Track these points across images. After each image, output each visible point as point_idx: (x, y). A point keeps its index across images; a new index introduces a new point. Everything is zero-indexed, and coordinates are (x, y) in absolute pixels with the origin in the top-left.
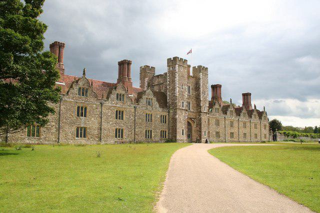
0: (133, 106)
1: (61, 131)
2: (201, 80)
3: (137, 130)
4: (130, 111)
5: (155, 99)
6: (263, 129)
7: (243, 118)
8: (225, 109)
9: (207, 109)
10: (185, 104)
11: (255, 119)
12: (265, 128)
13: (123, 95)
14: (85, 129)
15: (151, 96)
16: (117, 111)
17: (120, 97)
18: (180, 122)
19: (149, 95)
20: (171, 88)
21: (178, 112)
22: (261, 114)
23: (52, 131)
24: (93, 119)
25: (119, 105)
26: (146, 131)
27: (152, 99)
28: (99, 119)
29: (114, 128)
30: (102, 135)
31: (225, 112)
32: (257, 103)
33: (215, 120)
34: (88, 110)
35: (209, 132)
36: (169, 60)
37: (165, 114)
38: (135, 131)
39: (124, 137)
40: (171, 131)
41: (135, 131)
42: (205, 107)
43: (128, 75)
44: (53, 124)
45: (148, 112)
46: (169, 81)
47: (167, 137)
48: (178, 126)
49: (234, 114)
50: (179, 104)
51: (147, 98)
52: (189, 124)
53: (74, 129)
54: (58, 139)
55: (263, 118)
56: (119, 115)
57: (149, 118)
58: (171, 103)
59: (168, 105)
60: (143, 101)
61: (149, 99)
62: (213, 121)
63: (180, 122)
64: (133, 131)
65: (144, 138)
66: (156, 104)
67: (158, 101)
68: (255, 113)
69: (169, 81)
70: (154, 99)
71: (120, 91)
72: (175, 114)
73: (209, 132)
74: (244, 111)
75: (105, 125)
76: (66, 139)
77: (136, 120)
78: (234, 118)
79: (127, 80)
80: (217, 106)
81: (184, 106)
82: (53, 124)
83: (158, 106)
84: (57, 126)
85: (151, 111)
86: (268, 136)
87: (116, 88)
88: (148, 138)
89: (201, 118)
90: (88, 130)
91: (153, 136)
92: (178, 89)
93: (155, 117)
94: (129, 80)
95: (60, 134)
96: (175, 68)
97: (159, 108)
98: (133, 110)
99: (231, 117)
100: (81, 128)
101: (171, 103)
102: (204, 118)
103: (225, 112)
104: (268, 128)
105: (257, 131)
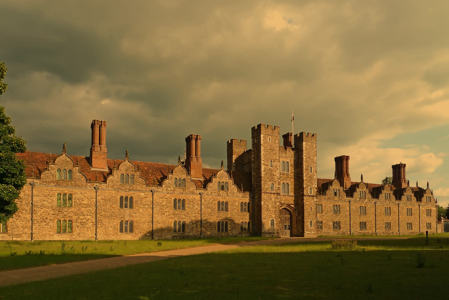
0: (198, 191)
1: (99, 226)
2: (304, 152)
4: (194, 199)
11: (408, 202)
17: (181, 184)
19: (221, 177)
22: (419, 193)
25: (178, 190)
34: (134, 200)
42: (310, 188)
44: (89, 217)
53: (117, 222)
55: (424, 199)
66: (233, 188)
67: (237, 183)
68: (408, 193)
82: (89, 217)
84: (94, 221)
86: (434, 224)
87: (172, 172)
88: (222, 230)
89: (303, 204)
98: (198, 197)
101: (255, 186)
102: (309, 203)
105: (411, 219)
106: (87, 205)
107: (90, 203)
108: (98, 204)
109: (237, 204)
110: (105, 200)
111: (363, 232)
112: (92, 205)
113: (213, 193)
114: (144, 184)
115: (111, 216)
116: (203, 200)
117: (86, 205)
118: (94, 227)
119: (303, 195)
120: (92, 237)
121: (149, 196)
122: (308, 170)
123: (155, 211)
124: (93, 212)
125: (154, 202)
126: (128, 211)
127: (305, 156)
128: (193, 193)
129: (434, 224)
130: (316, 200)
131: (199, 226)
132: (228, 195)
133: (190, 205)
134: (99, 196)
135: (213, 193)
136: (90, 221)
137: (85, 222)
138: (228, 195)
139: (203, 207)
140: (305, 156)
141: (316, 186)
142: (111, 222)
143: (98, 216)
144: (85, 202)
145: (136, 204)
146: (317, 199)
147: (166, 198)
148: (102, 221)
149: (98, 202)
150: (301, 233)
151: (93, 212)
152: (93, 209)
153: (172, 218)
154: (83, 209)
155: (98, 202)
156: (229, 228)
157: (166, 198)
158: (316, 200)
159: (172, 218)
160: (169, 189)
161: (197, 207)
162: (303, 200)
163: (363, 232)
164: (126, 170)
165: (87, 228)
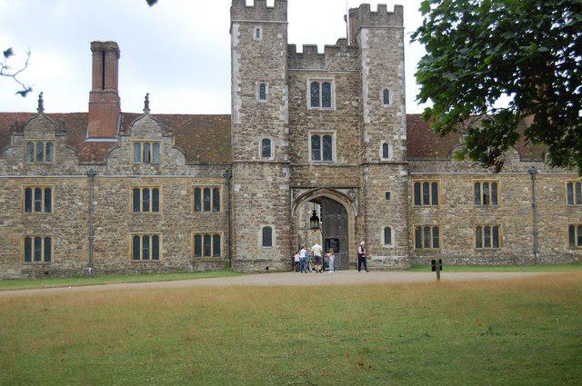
0: (84, 170)
5: (171, 142)
13: (49, 145)
16: (28, 191)
26: (136, 239)
27: (156, 144)
29: (20, 238)
37: (211, 183)
45: (141, 184)
51: (137, 144)
57: (145, 200)
61: (147, 144)
64: (85, 241)
65: (128, 258)
77: (97, 209)
83: (181, 161)
85: (151, 180)
91: (162, 251)
93: (171, 196)
97: (187, 167)
113: (123, 172)
128: (70, 172)
131: (85, 247)
132: (159, 173)
135: (123, 172)
141: (404, 137)
147: (7, 189)
153: (20, 231)
156: (165, 251)
157: (7, 189)
159: (20, 231)
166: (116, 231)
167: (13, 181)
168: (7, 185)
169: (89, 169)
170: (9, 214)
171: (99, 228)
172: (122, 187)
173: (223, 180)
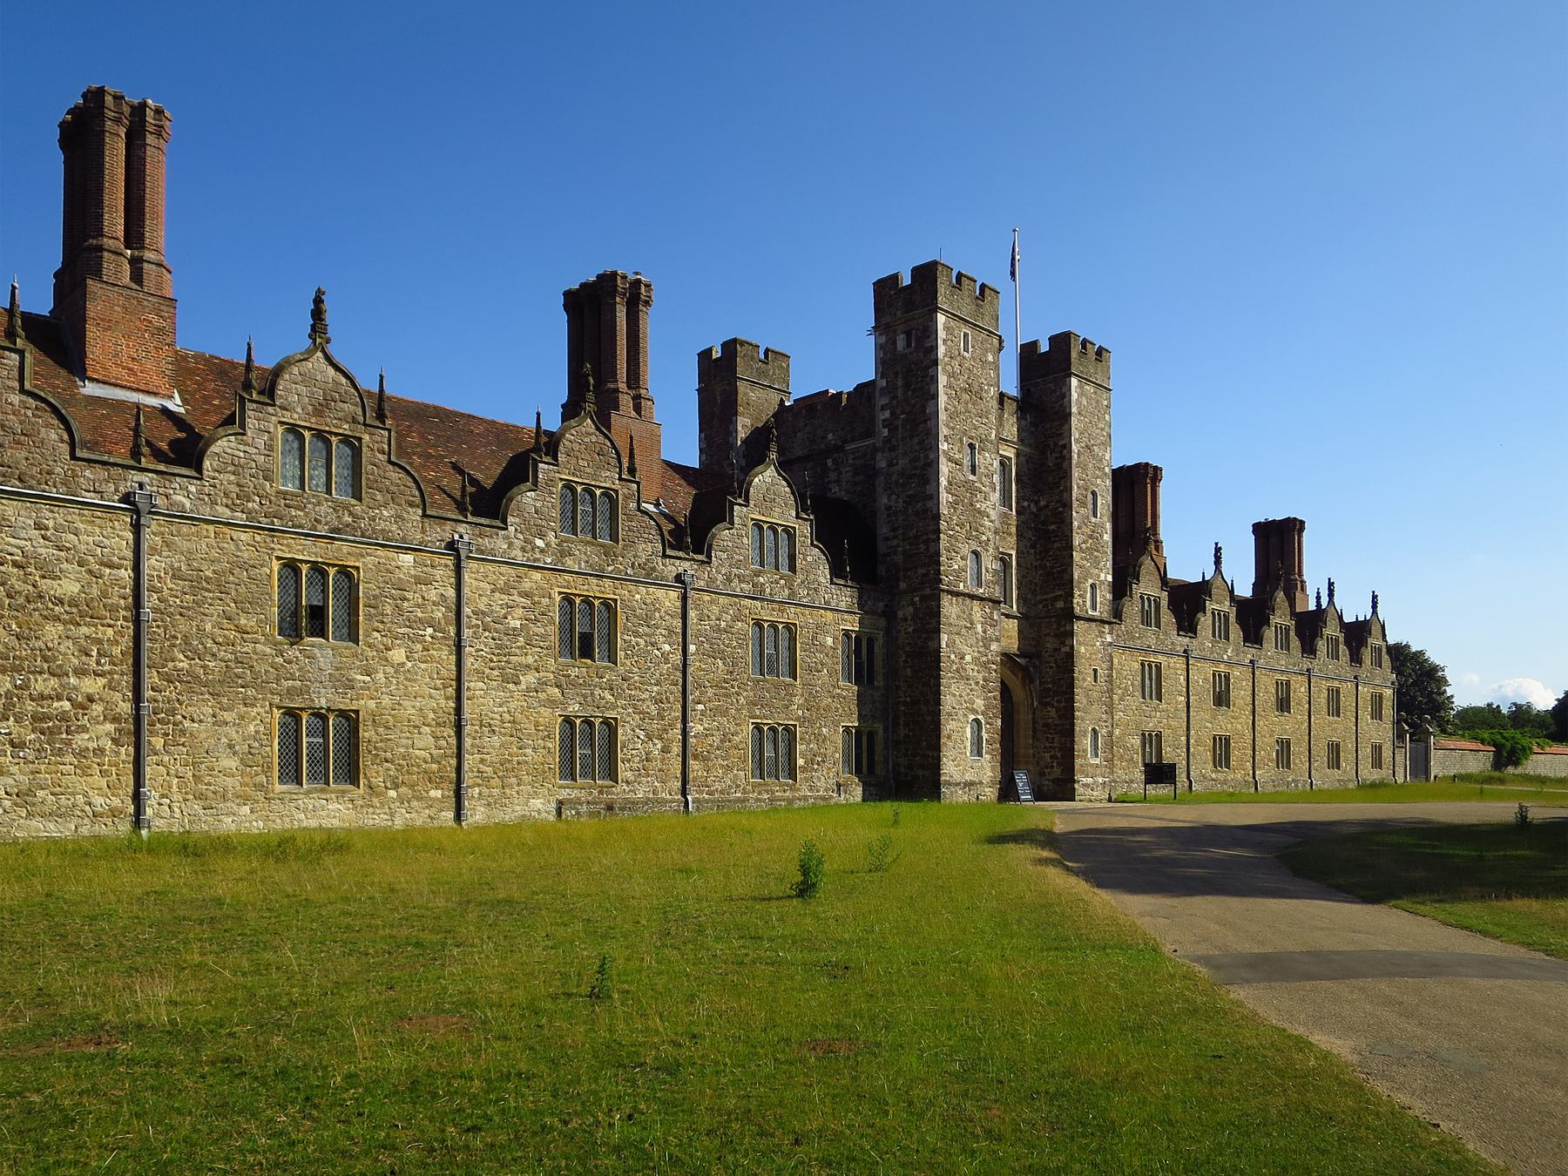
0: (671, 569)
1: (158, 742)
2: (1074, 420)
3: (696, 728)
4: (655, 605)
6: (1365, 715)
7: (1278, 658)
8: (1188, 602)
9: (1104, 595)
10: (990, 564)
11: (1330, 666)
12: (1377, 714)
14: (351, 720)
15: (784, 512)
18: (961, 675)
19: (768, 501)
20: (903, 462)
21: (950, 609)
22: (1358, 634)
23: (80, 740)
24: (398, 655)
25: (582, 555)
28: (447, 656)
29: (551, 718)
30: (470, 760)
31: (1187, 626)
32: (1333, 572)
33: (1137, 666)
35: (1110, 734)
36: (886, 290)
38: (684, 732)
39: (624, 772)
40: (902, 732)
41: (684, 732)
43: (634, 378)
44: (91, 685)
46: (887, 424)
47: (879, 770)
48: (948, 702)
49: (1236, 632)
50: (956, 563)
51: (758, 525)
52: (1005, 691)
53: (259, 723)
54: (137, 797)
56: (587, 633)
58: (899, 559)
59: (882, 570)
60: (734, 540)
62: (1128, 666)
63: (961, 675)
66: (814, 560)
69: (887, 424)
70: (804, 530)
71: (582, 458)
72: (930, 622)
73: (1110, 734)
74: (1280, 618)
75: (483, 699)
76: (200, 796)
78: (1234, 648)
79: (626, 401)
80: (1147, 586)
81: (987, 577)
82: (91, 685)
83: (823, 573)
84: (125, 708)
90: (366, 733)
92: (945, 468)
94: (638, 408)
95: (150, 760)
96: (929, 331)
99: (1216, 648)
100: (319, 715)
101: (899, 559)
102: (1089, 645)
103: (1187, 626)
104: (1388, 711)
106: (82, 611)
107: (95, 592)
108: (150, 601)
109: (830, 641)
110: (196, 583)
111: (1221, 776)
112: (113, 609)
114: (411, 505)
115: (229, 679)
116: (692, 614)
117: (73, 603)
118: (127, 752)
119: (1069, 616)
120: (114, 813)
121: (438, 573)
122: (1083, 504)
123: (468, 662)
124: (116, 651)
125: (467, 610)
126: (323, 653)
127: (1077, 441)
129: (1387, 753)
130: (1109, 639)
132: (792, 594)
133: (637, 634)
134: (154, 551)
136: (97, 708)
137: (63, 717)
138: (792, 594)
139: (692, 648)
140: (1077, 441)
141: (1110, 578)
142: (228, 716)
143: (151, 677)
144: (69, 587)
145: (369, 617)
146: (1111, 633)
147: (526, 595)
148: (173, 712)
149: (153, 589)
150: (1056, 781)
151: (116, 651)
152: (115, 634)
153: (551, 703)
154: (52, 631)
155: (153, 589)
158: (1109, 639)
159: (551, 703)
160: (540, 543)
161: (667, 647)
162: (1071, 634)
163: (1221, 776)
164: (318, 412)
165: (82, 753)
166: (725, 713)
167: (537, 576)
168: (527, 585)
169: (681, 570)
170: (530, 660)
171: (700, 707)
172: (736, 618)
173: (882, 623)
